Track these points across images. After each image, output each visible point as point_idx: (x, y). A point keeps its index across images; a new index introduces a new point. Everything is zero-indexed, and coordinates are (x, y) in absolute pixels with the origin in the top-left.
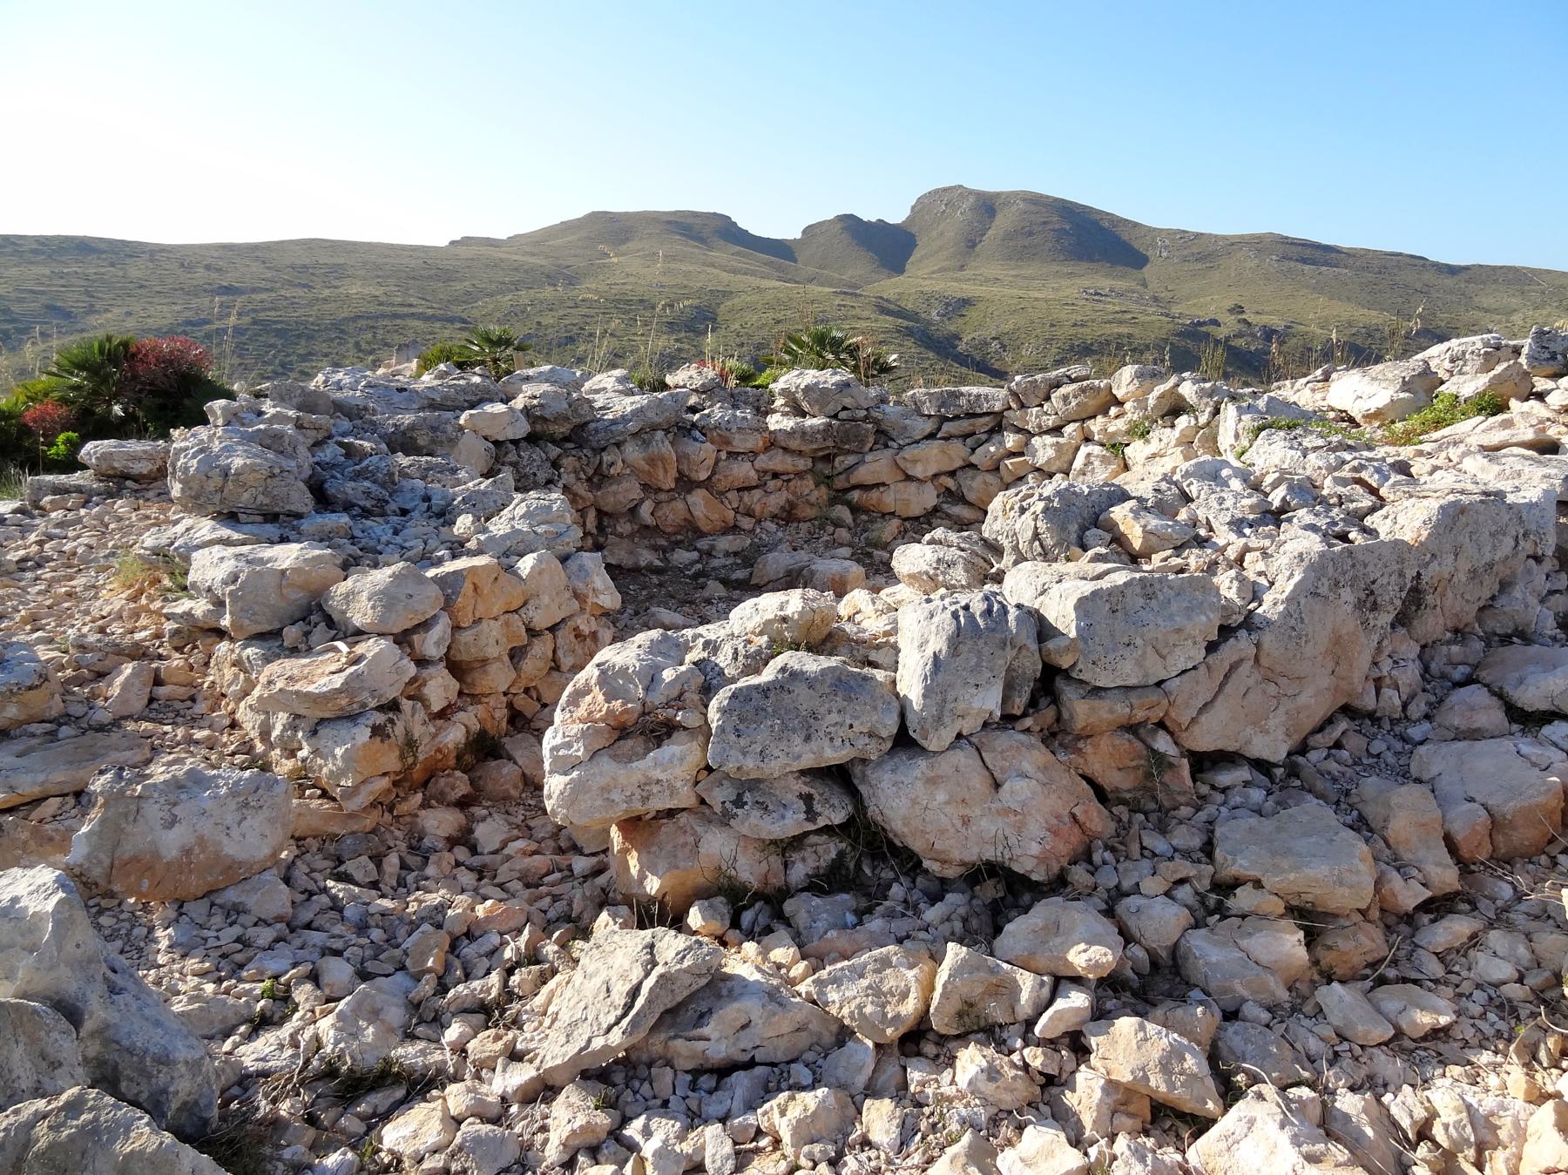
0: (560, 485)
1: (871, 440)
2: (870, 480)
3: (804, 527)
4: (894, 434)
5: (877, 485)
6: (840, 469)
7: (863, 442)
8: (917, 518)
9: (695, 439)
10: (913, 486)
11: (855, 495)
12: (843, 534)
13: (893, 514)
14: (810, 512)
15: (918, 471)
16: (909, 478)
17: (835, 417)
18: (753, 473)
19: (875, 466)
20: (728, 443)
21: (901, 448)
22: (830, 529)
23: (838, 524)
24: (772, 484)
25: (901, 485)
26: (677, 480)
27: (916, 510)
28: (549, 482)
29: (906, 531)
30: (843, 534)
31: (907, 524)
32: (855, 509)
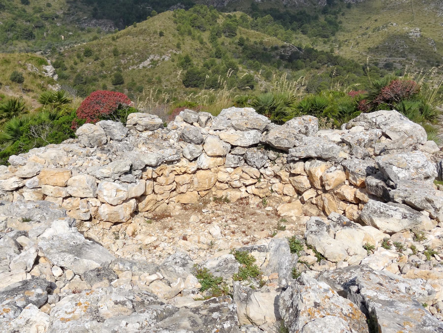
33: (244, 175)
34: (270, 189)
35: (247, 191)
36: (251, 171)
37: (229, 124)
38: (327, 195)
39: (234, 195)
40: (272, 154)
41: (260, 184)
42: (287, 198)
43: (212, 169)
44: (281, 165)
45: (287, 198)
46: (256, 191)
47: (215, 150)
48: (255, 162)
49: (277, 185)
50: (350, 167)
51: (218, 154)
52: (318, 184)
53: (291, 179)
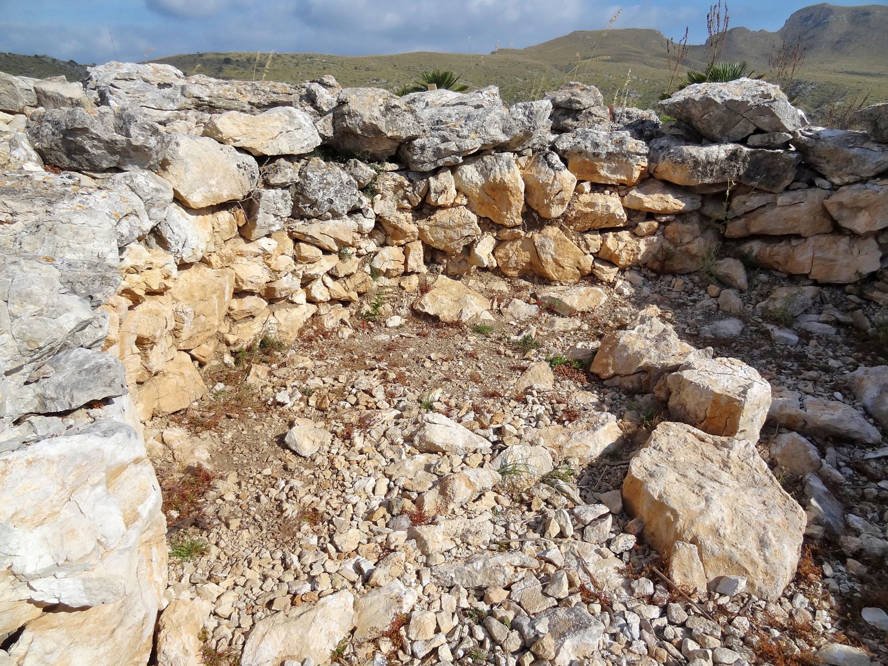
0: (371, 213)
1: (791, 176)
2: (779, 229)
3: (678, 283)
4: (827, 168)
5: (787, 237)
6: (739, 211)
7: (778, 179)
8: (841, 286)
9: (551, 166)
10: (843, 243)
11: (755, 247)
12: (732, 299)
13: (806, 276)
14: (691, 265)
15: (861, 223)
16: (837, 229)
17: (744, 142)
18: (621, 212)
19: (792, 209)
20: (595, 172)
21: (835, 188)
22: (714, 289)
23: (724, 282)
24: (644, 226)
25: (823, 239)
26: (524, 215)
27: (844, 275)
28: (354, 211)
29: (823, 302)
30: (732, 299)
31: (826, 293)
32: (752, 265)
33: (308, 250)
34: (367, 269)
35: (311, 300)
36: (326, 231)
37: (183, 101)
38: (552, 231)
39: (289, 320)
40: (366, 171)
41: (349, 263)
42: (414, 280)
43: (214, 259)
44: (390, 194)
45: (414, 280)
46: (337, 288)
47: (213, 182)
48: (331, 202)
49: (389, 257)
50: (596, 145)
51: (225, 197)
52: (514, 216)
53: (423, 223)
